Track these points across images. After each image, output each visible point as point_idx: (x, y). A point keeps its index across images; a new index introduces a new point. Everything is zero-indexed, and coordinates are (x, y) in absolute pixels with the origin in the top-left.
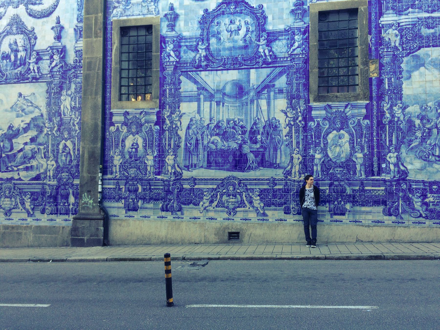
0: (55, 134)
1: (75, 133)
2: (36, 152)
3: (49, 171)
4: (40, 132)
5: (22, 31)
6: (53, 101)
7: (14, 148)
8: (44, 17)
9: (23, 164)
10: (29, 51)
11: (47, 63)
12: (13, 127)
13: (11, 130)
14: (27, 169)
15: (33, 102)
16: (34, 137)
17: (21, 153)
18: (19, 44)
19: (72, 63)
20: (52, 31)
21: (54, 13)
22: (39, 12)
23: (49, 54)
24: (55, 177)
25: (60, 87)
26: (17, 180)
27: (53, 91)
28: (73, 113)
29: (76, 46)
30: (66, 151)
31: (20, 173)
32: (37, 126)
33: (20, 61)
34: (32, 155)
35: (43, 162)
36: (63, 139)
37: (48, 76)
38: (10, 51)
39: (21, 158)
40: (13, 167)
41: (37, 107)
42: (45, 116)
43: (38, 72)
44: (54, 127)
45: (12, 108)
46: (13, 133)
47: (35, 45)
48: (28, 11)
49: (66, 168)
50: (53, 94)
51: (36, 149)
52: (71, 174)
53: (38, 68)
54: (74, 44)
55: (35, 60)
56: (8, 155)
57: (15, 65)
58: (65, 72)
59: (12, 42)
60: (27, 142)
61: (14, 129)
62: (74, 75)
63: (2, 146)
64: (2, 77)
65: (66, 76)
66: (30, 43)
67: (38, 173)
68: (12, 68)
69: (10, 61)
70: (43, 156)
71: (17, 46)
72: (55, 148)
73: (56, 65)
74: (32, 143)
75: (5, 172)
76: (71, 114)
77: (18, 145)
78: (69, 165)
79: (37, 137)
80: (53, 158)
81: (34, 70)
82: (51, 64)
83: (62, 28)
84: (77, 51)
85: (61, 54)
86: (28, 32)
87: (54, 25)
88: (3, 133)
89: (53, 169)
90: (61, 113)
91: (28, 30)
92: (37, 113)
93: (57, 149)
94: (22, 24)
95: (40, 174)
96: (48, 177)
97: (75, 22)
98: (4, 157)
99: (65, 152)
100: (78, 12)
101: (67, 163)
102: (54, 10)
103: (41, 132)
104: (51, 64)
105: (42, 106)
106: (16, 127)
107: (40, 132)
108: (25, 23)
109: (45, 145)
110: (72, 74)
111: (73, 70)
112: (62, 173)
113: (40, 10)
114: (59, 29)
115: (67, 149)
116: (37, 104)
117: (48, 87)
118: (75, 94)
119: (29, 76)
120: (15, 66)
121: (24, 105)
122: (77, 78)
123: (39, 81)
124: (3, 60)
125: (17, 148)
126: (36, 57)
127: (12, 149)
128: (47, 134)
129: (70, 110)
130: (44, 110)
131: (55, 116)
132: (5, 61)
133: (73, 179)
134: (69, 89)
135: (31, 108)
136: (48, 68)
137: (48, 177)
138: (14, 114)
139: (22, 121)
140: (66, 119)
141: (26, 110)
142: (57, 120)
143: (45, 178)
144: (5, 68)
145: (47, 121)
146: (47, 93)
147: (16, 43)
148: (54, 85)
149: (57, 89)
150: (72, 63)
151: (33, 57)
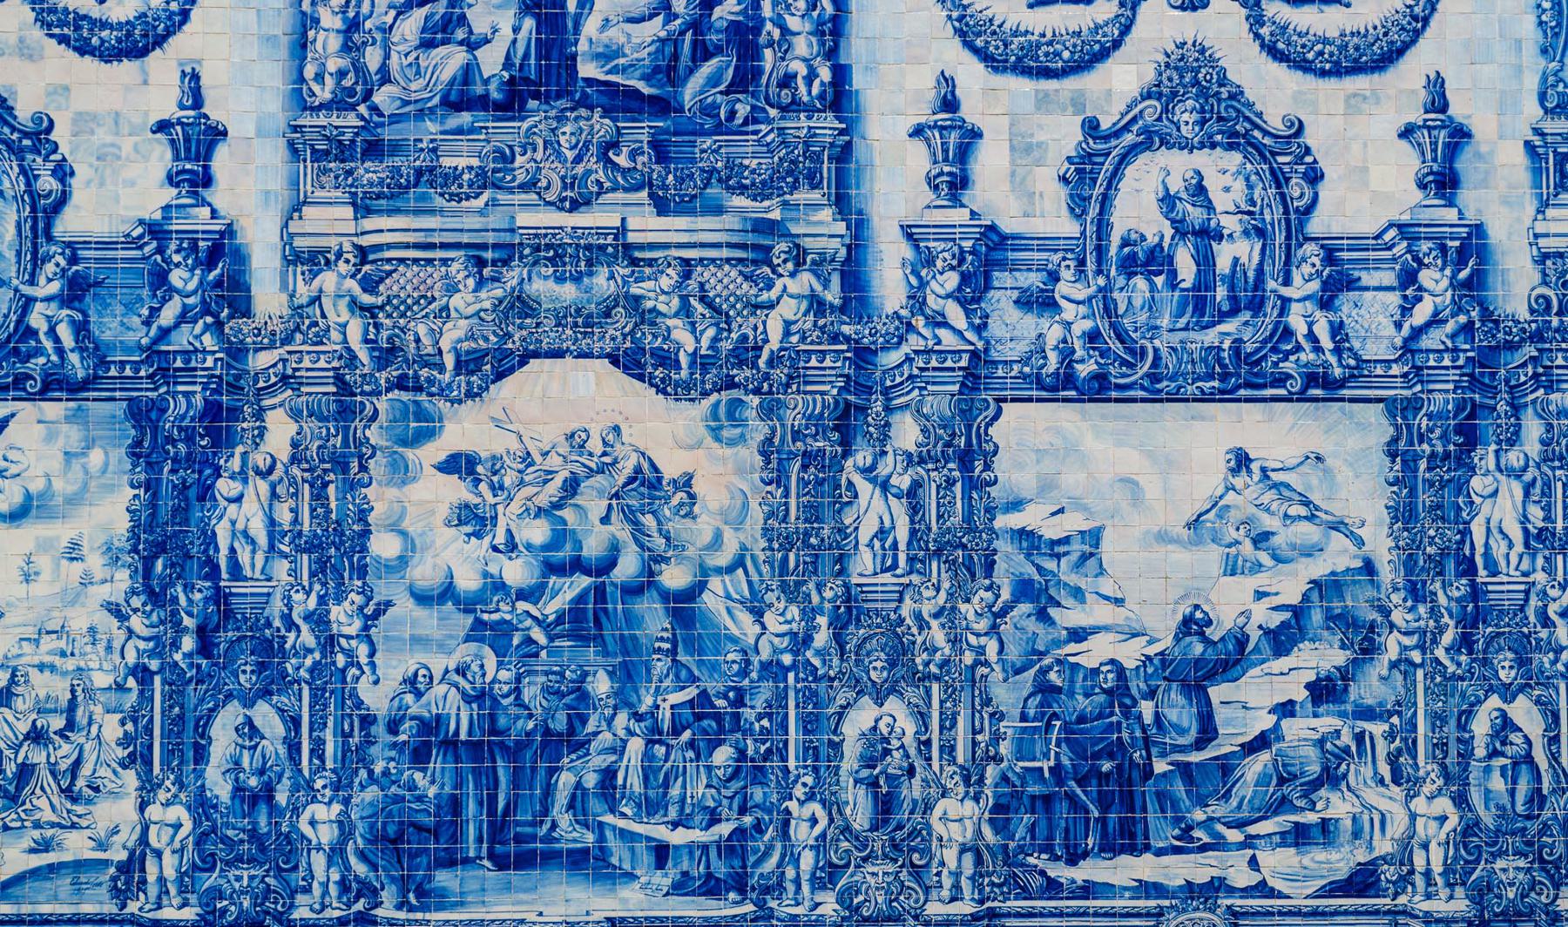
0: (1447, 662)
1: (1556, 661)
2: (1347, 750)
3: (1425, 846)
4: (1364, 651)
5: (1236, 134)
6: (1425, 498)
7: (1221, 731)
8: (1357, 69)
9: (1276, 813)
10: (1280, 238)
11: (1386, 306)
12: (1209, 623)
13: (1195, 638)
14: (1299, 836)
15: (1316, 498)
16: (1328, 678)
17: (1265, 757)
18: (1221, 201)
19: (1523, 314)
20: (1404, 143)
21: (1410, 55)
22: (1325, 41)
23: (1394, 259)
24: (1455, 875)
25: (1459, 430)
26: (1247, 892)
27: (1425, 446)
28: (1540, 561)
29: (1540, 227)
30: (1508, 750)
31: (1260, 856)
32: (1342, 621)
33: (1232, 288)
34: (1326, 769)
35: (1389, 800)
36: (1490, 690)
37: (1396, 370)
38: (1169, 232)
39: (1263, 780)
40: (1220, 828)
41: (1337, 526)
42: (1387, 574)
43: (1338, 351)
44: (1441, 630)
45: (1195, 523)
46: (1211, 654)
47: (1309, 210)
48: (1265, 31)
49: (1513, 833)
50: (1423, 465)
51: (1346, 739)
52: (1542, 861)
53: (1337, 330)
54: (1528, 223)
55: (1315, 286)
56: (1189, 764)
57: (1199, 304)
58: (1487, 358)
59: (1176, 185)
60: (1291, 702)
61: (1214, 633)
62: (1536, 376)
63: (1148, 718)
64: (1131, 366)
65: (1493, 375)
66: (1283, 196)
67: (1362, 856)
68: (1182, 322)
69: (1174, 287)
70: (1385, 770)
71: (1210, 207)
72: (1451, 728)
73: (1435, 321)
74: (1321, 710)
75: (1177, 851)
76: (1525, 566)
77: (1241, 713)
78: (1528, 817)
79: (1346, 674)
80: (1440, 782)
81: (1312, 337)
82: (1406, 311)
83: (1461, 134)
84: (1544, 257)
85: (1461, 261)
86: (1267, 141)
87: (1416, 116)
88: (1152, 650)
89: (1443, 836)
90: (1472, 560)
91: (1266, 133)
92: (1338, 557)
93: (1459, 740)
94: (1232, 97)
95: (1373, 862)
96: (1419, 881)
97: (1533, 110)
98: (1164, 775)
99: (1503, 754)
100: (1542, 62)
101: (1520, 808)
102: (1413, 42)
103: (1369, 649)
104: (1406, 311)
105: (1370, 519)
106: (1228, 624)
107: (1364, 651)
108: (1250, 95)
109: (1395, 720)
110: (1524, 365)
111: (1530, 350)
112: (1495, 856)
113: (1333, 33)
114: (1443, 136)
115: (1516, 738)
116: (1338, 509)
117: (1397, 427)
118: (1545, 469)
119: (1288, 366)
120: (1200, 308)
121: (1268, 510)
122: (1550, 388)
123: (1346, 392)
124: (1130, 275)
125: (1235, 729)
126: (1319, 274)
127: (1207, 732)
128: (1403, 665)
129: (1519, 547)
130: (1381, 545)
131: (1441, 574)
132: (1140, 282)
133: (1557, 886)
134: (1514, 439)
135: (1307, 532)
136: (1391, 330)
137: (1419, 881)
138: (1212, 556)
139: (1260, 595)
140: (1503, 587)
141: (1276, 541)
142: (1456, 594)
143: (1405, 880)
144: (1143, 318)
145: (1396, 598)
146: (1393, 455)
147: (1199, 190)
148: (1430, 416)
149: (1444, 437)
150: (1523, 314)
151: (1307, 269)
